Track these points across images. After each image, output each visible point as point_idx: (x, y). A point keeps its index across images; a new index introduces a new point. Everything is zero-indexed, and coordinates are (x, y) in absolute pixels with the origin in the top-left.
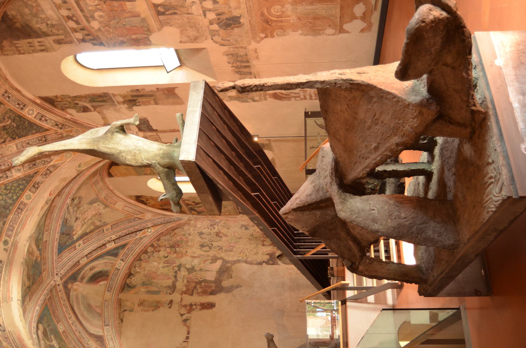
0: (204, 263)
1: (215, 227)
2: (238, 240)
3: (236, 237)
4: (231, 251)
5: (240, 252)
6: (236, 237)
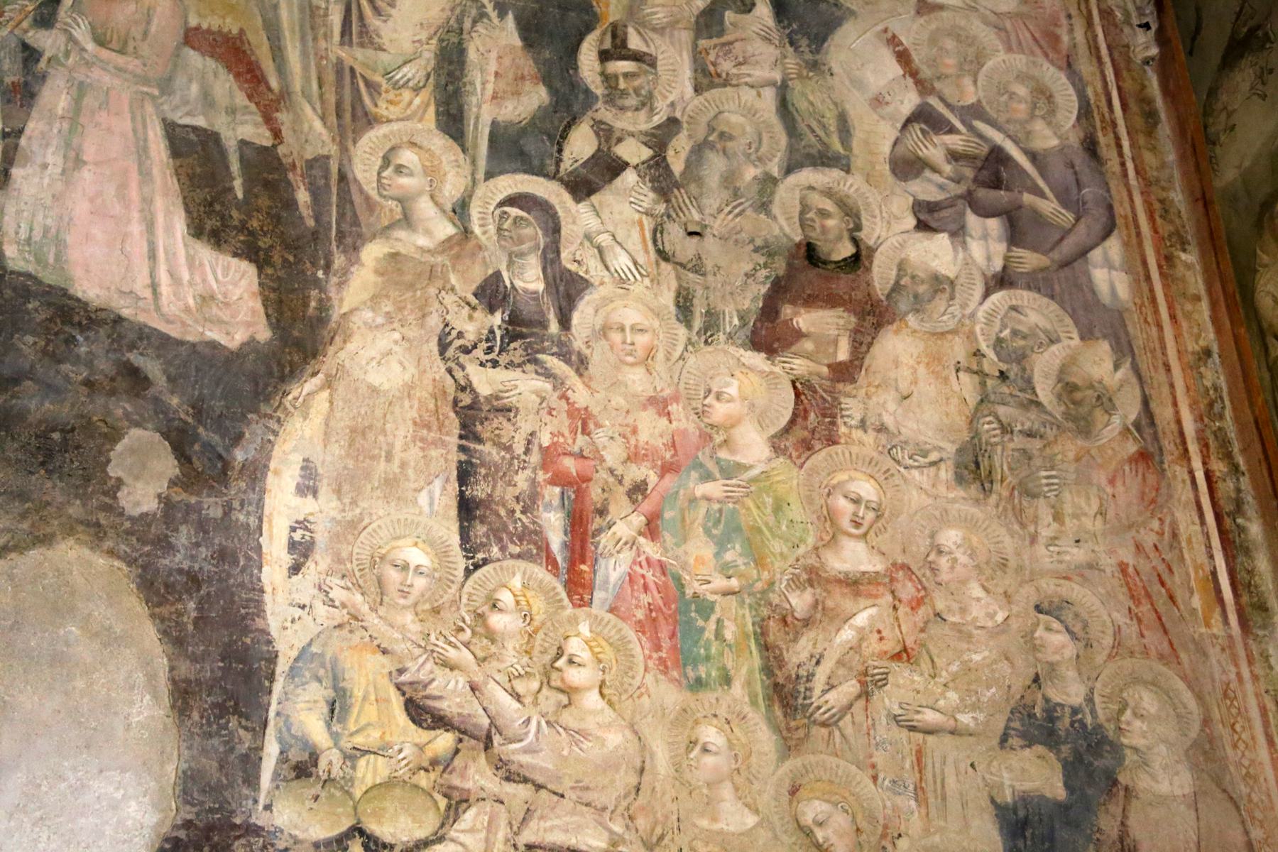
0: (192, 37)
1: (958, 233)
2: (748, 665)
3: (792, 624)
4: (467, 509)
5: (447, 707)
6: (792, 624)
